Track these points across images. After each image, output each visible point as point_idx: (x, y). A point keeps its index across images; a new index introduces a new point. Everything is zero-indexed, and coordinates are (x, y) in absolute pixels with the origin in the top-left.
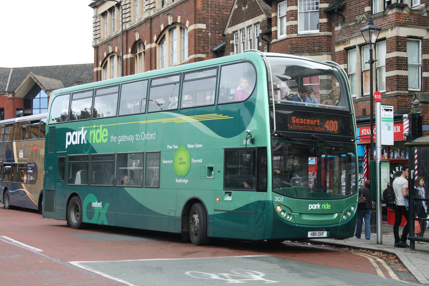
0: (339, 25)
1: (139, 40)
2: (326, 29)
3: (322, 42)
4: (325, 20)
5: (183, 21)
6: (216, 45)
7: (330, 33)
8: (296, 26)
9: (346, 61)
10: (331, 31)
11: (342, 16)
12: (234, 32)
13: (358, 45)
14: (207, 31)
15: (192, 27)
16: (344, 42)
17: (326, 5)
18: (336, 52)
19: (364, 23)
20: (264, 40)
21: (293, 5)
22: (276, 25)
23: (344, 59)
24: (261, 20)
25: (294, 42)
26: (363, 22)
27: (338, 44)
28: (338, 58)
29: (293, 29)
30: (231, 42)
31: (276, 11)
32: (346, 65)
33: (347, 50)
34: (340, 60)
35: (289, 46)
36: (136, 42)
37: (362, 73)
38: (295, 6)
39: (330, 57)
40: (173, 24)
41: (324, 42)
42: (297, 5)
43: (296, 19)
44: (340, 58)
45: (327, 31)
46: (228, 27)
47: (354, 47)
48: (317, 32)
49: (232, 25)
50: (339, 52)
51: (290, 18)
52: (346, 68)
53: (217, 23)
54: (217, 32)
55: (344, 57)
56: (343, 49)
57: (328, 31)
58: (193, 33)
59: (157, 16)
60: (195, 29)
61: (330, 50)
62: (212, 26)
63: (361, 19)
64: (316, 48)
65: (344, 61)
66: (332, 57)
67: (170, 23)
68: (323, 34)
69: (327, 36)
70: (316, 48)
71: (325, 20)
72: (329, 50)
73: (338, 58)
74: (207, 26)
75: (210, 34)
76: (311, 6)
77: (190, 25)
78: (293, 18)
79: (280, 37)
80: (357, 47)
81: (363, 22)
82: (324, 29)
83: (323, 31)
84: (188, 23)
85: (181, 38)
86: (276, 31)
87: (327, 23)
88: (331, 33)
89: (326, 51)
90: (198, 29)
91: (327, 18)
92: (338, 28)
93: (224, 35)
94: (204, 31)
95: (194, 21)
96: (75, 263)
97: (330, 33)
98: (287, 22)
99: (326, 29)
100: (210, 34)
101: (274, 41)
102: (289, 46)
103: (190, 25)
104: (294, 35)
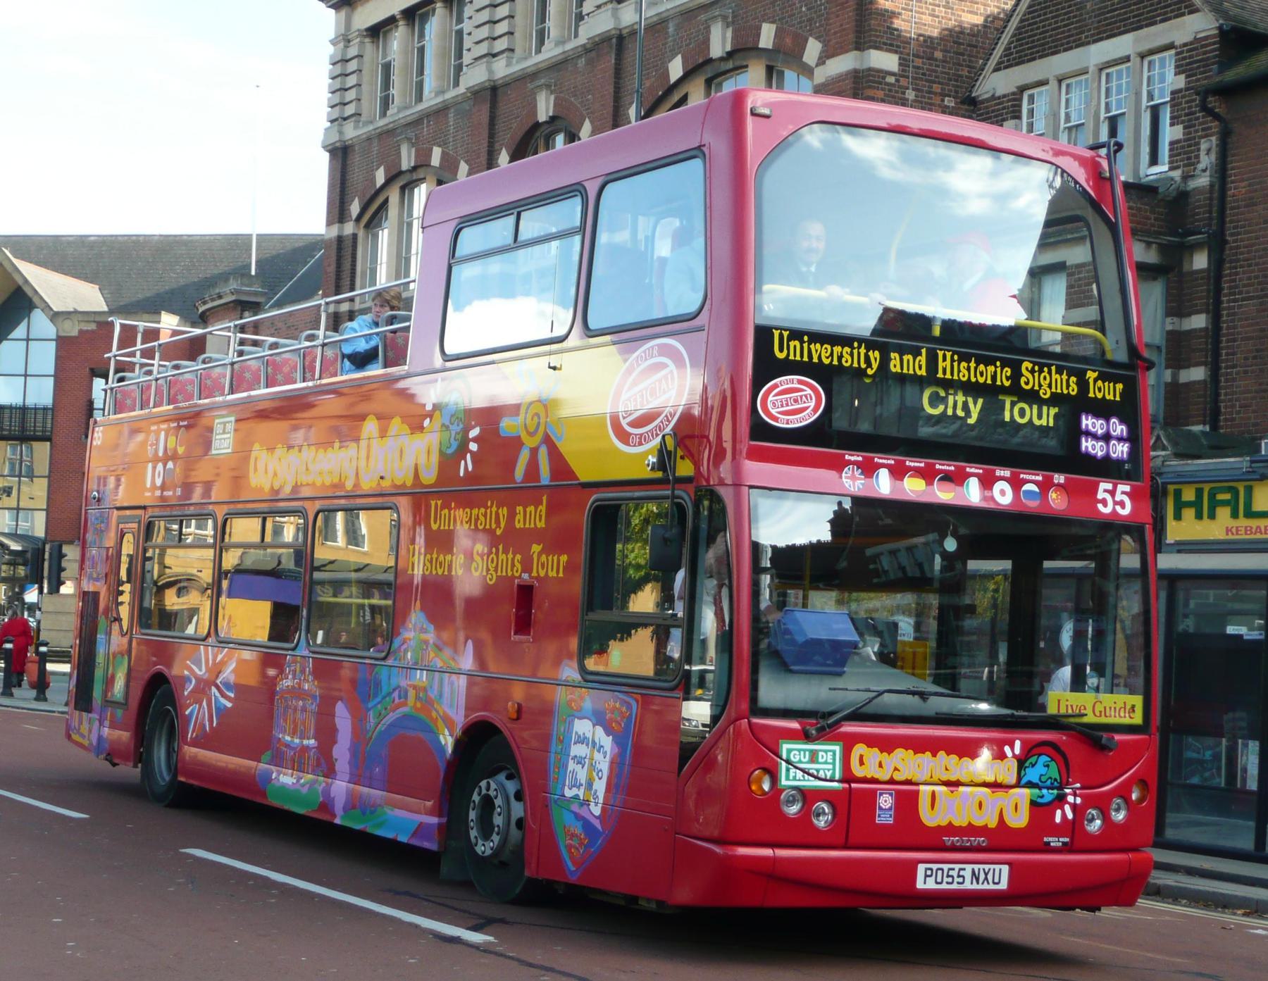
1: (553, 119)
5: (788, 41)
12: (1022, 89)
14: (903, 82)
36: (537, 125)
40: (730, 55)
46: (996, 70)
49: (1013, 59)
53: (938, 55)
54: (936, 88)
59: (657, 27)
60: (856, 71)
62: (918, 62)
67: (716, 50)
74: (903, 63)
84: (813, 50)
90: (870, 69)
94: (891, 80)
95: (852, 37)
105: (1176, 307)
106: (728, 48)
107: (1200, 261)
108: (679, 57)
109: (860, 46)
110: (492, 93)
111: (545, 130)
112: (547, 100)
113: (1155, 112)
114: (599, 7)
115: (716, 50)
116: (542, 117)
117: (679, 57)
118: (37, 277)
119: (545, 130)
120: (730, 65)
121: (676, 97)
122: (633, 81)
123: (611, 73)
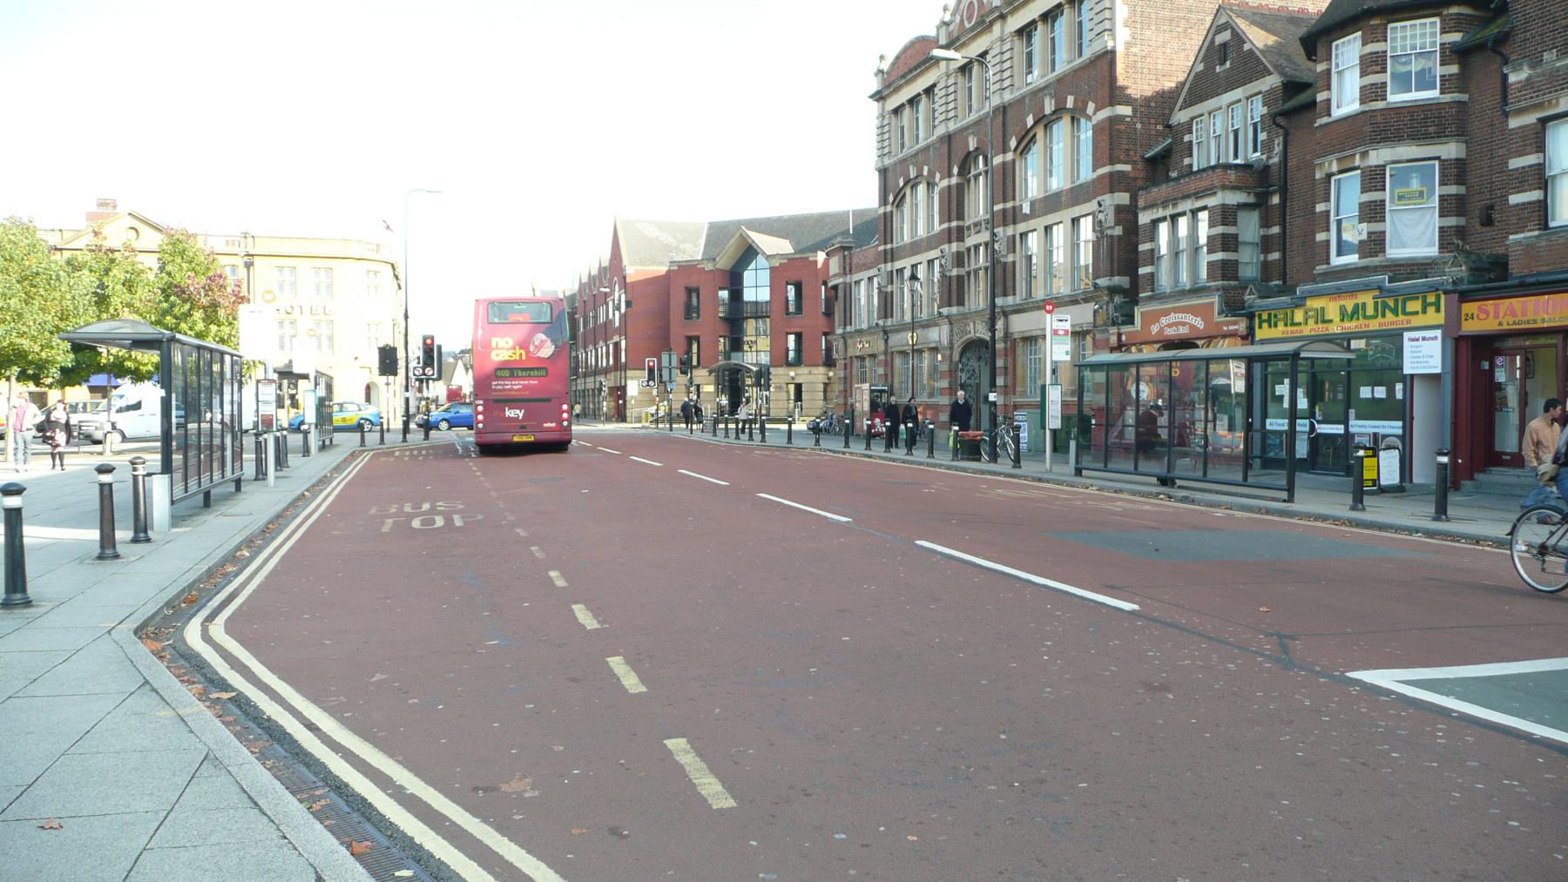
0: (1525, 68)
4: (1454, 69)
6: (1150, 147)
7: (1464, 97)
8: (1384, 84)
9: (1541, 147)
11: (1502, 55)
12: (1192, 119)
15: (1104, 114)
16: (1539, 106)
17: (1456, 37)
20: (1278, 125)
22: (1329, 88)
24: (1265, 88)
25: (1379, 119)
27: (1520, 112)
29: (1371, 93)
30: (1186, 138)
31: (1329, 59)
33: (1544, 121)
35: (1368, 129)
39: (1464, 146)
43: (1384, 71)
48: (1433, 94)
49: (1188, 104)
58: (1107, 125)
59: (1020, 101)
64: (1432, 129)
67: (1048, 111)
68: (1448, 98)
69: (1459, 102)
70: (1432, 129)
71: (1454, 69)
72: (1461, 133)
74: (1134, 110)
75: (1139, 126)
77: (1097, 110)
79: (1337, 113)
84: (1091, 107)
85: (1073, 137)
86: (1329, 101)
93: (1169, 126)
97: (1464, 97)
100: (1139, 126)
101: (1325, 120)
102: (1368, 129)
103: (1097, 110)
104: (1380, 105)
105: (1265, 223)
107: (1276, 200)
109: (1111, 105)
110: (948, 138)
113: (1255, 125)
115: (1048, 111)
118: (759, 239)
122: (1010, 128)
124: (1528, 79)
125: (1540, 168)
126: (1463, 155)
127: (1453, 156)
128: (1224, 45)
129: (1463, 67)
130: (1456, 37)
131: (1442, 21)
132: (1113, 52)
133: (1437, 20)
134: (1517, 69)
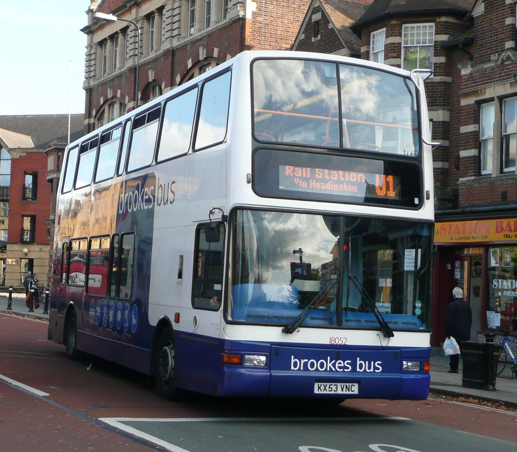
0: (469, 66)
1: (154, 81)
2: (443, 72)
3: (436, 92)
4: (442, 60)
5: (222, 55)
7: (449, 79)
9: (477, 120)
10: (449, 76)
11: (469, 53)
13: (498, 97)
16: (475, 93)
17: (444, 38)
18: (462, 107)
19: (508, 65)
21: (395, 36)
23: (474, 117)
26: (507, 63)
27: (467, 95)
28: (465, 116)
31: (368, 44)
32: (477, 125)
33: (479, 103)
34: (468, 118)
36: (149, 83)
37: (502, 139)
38: (398, 38)
39: (447, 113)
40: (206, 59)
41: (440, 92)
42: (401, 36)
43: (399, 56)
44: (468, 115)
45: (445, 76)
47: (492, 100)
50: (466, 106)
51: (390, 55)
52: (478, 130)
55: (475, 114)
56: (474, 102)
57: (447, 76)
59: (184, 47)
61: (449, 103)
63: (505, 58)
65: (475, 120)
66: (450, 114)
67: (201, 58)
68: (438, 79)
69: (445, 83)
71: (442, 60)
73: (465, 116)
76: (428, 38)
78: (395, 55)
80: (496, 99)
81: (507, 63)
82: (440, 72)
83: (439, 75)
87: (444, 63)
88: (451, 78)
89: (442, 105)
91: (445, 56)
92: (465, 72)
96: (112, 422)
97: (449, 79)
98: (385, 59)
99: (443, 72)
106: (205, 57)
108: (190, 60)
110: (134, 70)
111: (152, 84)
112: (152, 73)
114: (166, 39)
115: (201, 58)
116: (150, 80)
117: (190, 60)
119: (152, 84)
120: (206, 63)
121: (190, 74)
122: (177, 67)
123: (170, 64)
124: (471, 74)
125: (476, 134)
126: (447, 119)
127: (441, 119)
128: (317, 22)
129: (448, 58)
130: (444, 38)
131: (436, 26)
132: (243, 19)
133: (433, 24)
134: (465, 67)
